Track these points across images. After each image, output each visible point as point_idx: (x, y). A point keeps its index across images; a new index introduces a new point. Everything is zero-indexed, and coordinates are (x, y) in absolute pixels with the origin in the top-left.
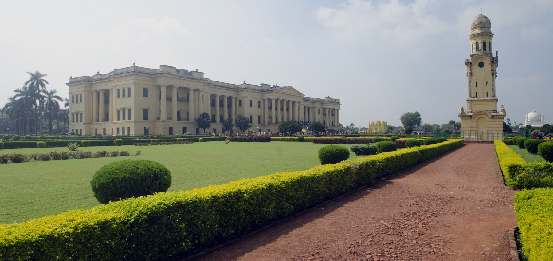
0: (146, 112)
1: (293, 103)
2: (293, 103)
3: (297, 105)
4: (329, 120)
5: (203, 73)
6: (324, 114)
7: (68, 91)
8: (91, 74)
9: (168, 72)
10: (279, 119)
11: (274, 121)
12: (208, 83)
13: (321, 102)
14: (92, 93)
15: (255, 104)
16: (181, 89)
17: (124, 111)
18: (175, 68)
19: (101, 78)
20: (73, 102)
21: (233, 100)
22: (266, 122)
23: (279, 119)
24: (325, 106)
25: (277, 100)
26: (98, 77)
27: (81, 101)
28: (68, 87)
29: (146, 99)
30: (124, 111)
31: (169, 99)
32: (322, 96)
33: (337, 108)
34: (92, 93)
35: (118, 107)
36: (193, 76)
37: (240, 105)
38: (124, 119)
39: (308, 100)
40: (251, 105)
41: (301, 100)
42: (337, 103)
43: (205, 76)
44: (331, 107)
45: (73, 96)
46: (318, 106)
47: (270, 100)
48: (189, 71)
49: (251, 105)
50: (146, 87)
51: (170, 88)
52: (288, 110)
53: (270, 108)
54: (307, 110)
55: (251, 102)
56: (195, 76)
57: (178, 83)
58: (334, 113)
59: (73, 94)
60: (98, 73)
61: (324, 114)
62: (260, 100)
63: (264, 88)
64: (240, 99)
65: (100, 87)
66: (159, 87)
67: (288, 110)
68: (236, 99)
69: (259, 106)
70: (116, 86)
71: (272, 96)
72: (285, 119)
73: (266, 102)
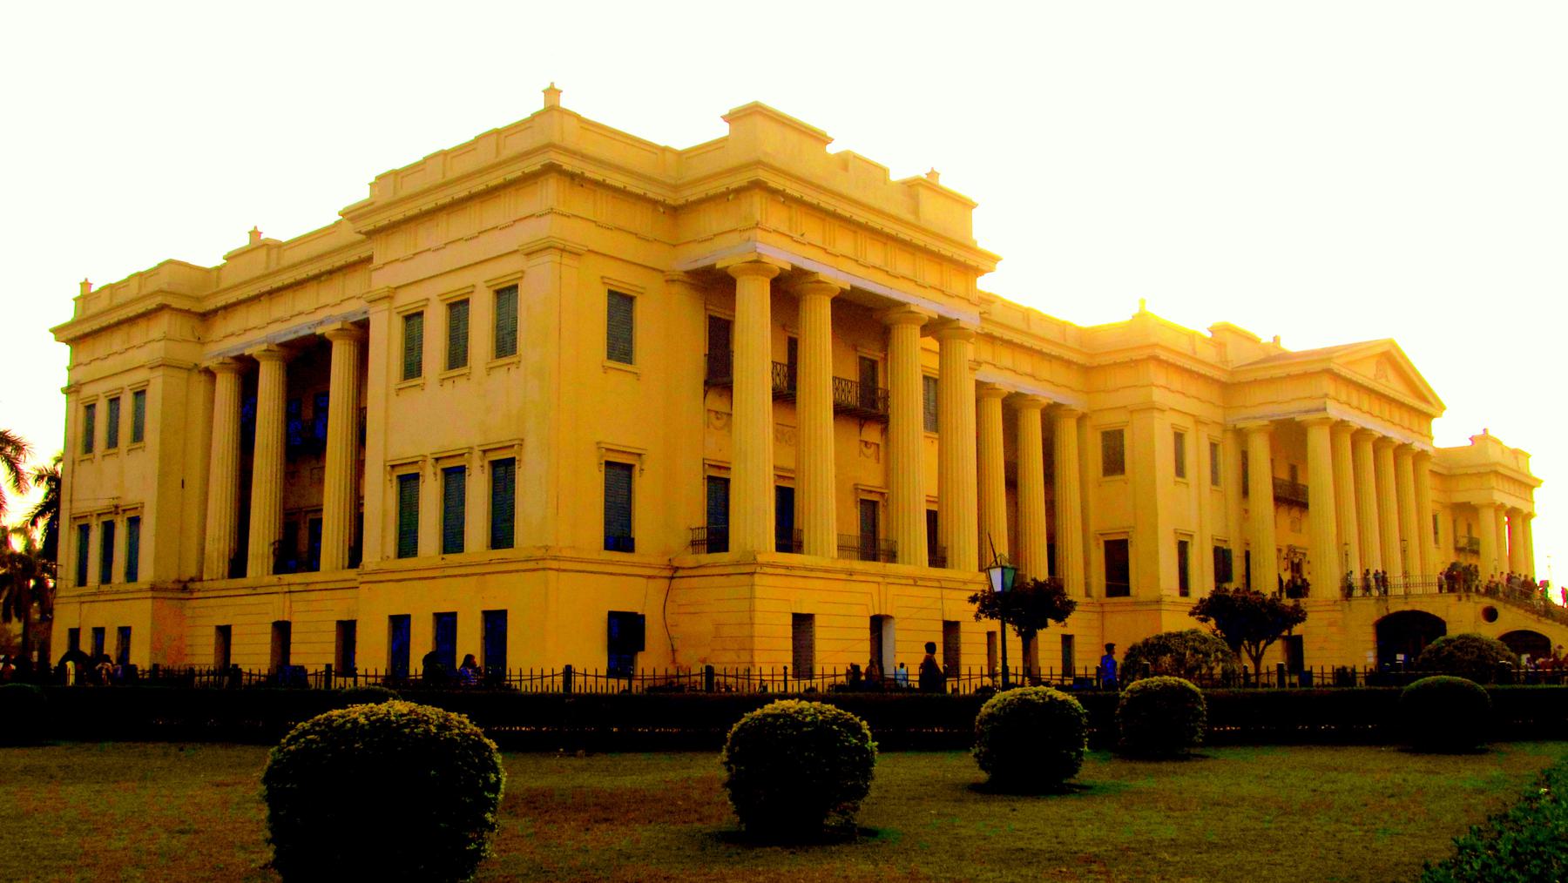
5: (968, 205)
7: (64, 380)
8: (208, 250)
14: (210, 374)
17: (454, 476)
18: (822, 139)
19: (272, 273)
20: (89, 447)
26: (258, 266)
27: (138, 435)
28: (65, 350)
29: (619, 378)
30: (454, 476)
35: (404, 449)
37: (1114, 463)
38: (453, 540)
40: (1180, 471)
45: (90, 408)
48: (896, 176)
49: (1180, 471)
50: (626, 280)
55: (1179, 437)
59: (88, 391)
60: (255, 234)
62: (1217, 434)
63: (1238, 356)
64: (1111, 420)
65: (258, 332)
68: (1081, 419)
69: (1215, 480)
70: (389, 297)
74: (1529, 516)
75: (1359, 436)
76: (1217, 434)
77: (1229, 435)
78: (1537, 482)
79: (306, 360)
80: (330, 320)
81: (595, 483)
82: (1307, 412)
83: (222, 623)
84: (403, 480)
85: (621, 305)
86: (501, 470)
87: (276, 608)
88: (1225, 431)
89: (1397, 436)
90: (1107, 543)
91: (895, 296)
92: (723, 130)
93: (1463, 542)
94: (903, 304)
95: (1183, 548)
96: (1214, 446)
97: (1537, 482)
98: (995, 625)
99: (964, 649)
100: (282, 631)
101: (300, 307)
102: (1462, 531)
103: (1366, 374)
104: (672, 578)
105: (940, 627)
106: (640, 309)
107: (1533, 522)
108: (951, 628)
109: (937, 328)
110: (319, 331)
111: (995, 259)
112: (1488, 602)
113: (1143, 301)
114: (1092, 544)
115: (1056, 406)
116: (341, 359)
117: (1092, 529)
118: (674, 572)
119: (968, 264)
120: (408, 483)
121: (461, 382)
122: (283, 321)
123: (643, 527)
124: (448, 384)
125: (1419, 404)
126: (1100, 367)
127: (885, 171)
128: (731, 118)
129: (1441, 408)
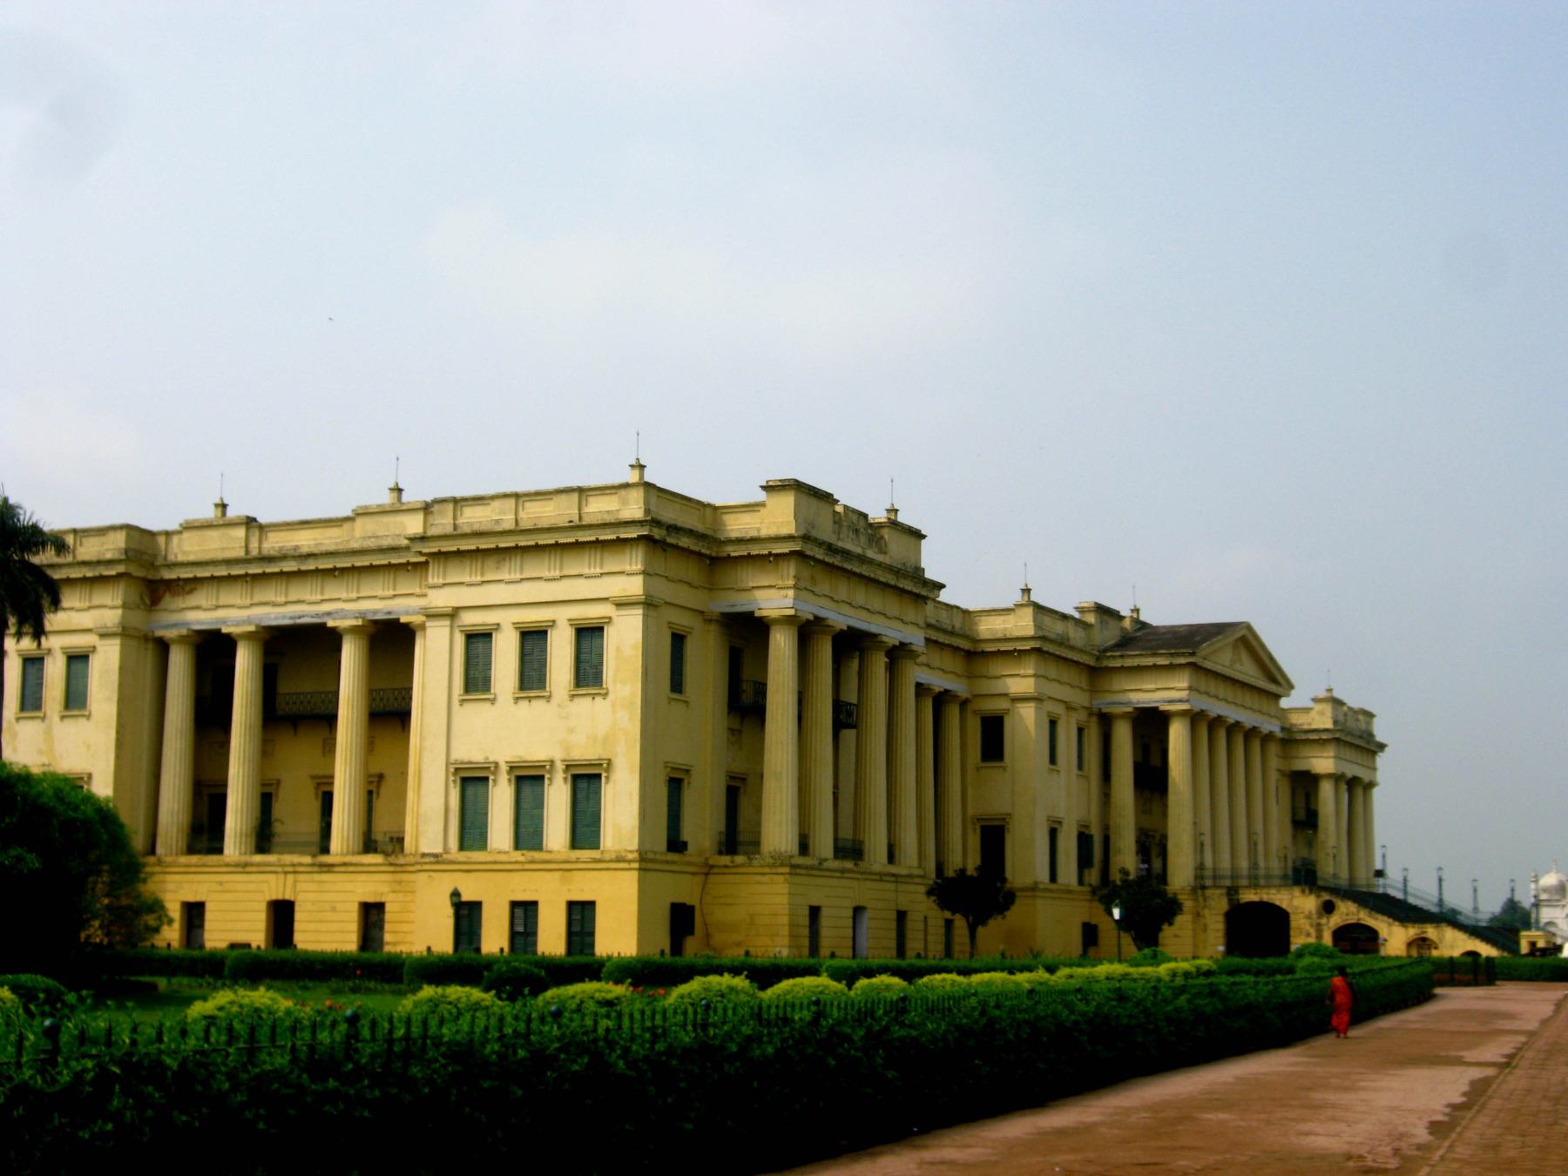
5: (918, 535)
14: (163, 647)
21: (953, 714)
33: (1366, 779)
34: (163, 647)
35: (470, 751)
38: (527, 833)
40: (1053, 759)
49: (1053, 759)
50: (683, 620)
56: (896, 549)
65: (238, 613)
68: (964, 704)
69: (1080, 766)
70: (453, 614)
73: (1123, 737)
74: (1371, 785)
75: (1215, 723)
76: (1082, 716)
77: (1094, 719)
78: (1382, 747)
79: (299, 649)
80: (342, 614)
81: (663, 791)
82: (1171, 702)
83: (191, 898)
84: (465, 781)
85: (678, 640)
86: (583, 785)
87: (276, 888)
88: (1091, 714)
89: (1248, 719)
90: (983, 828)
91: (873, 629)
92: (762, 496)
93: (1302, 815)
94: (876, 636)
95: (1053, 834)
96: (1080, 731)
97: (1382, 747)
98: (948, 915)
99: (909, 935)
100: (372, 914)
101: (308, 597)
102: (1301, 804)
103: (1222, 658)
104: (707, 874)
105: (894, 915)
106: (691, 647)
107: (1376, 792)
108: (901, 916)
109: (898, 654)
110: (331, 623)
111: (942, 586)
112: (1326, 897)
113: (1027, 591)
114: (969, 825)
115: (946, 691)
116: (351, 657)
117: (970, 812)
118: (708, 870)
119: (916, 589)
120: (472, 782)
121: (539, 705)
122: (275, 605)
123: (687, 834)
124: (524, 704)
125: (1272, 681)
126: (985, 654)
127: (865, 516)
128: (768, 488)
129: (1291, 687)
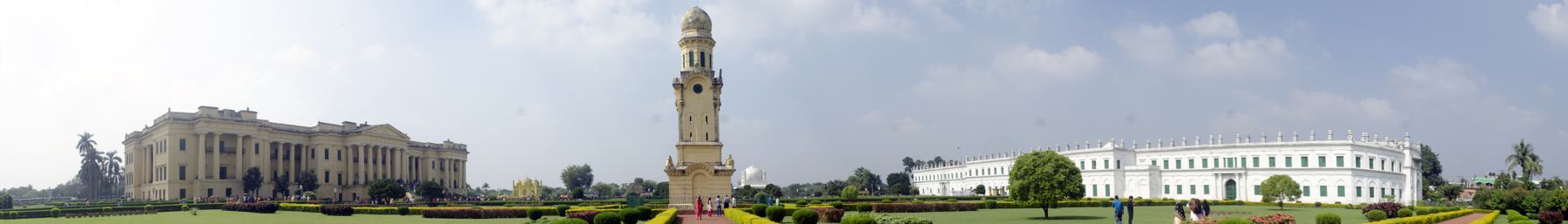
0: (182, 169)
1: (392, 151)
2: (392, 151)
3: (398, 154)
4: (449, 177)
6: (442, 169)
9: (209, 115)
10: (371, 177)
11: (362, 180)
12: (264, 126)
13: (437, 148)
15: (333, 154)
16: (225, 135)
22: (351, 182)
23: (371, 177)
24: (444, 156)
25: (366, 148)
31: (209, 151)
32: (438, 140)
36: (243, 118)
39: (416, 146)
41: (405, 147)
42: (462, 150)
43: (259, 117)
44: (451, 157)
46: (432, 156)
47: (356, 148)
51: (210, 136)
52: (384, 162)
53: (356, 160)
54: (415, 163)
56: (245, 117)
57: (219, 129)
58: (458, 166)
61: (442, 169)
66: (197, 136)
67: (384, 162)
71: (359, 141)
72: (380, 177)
